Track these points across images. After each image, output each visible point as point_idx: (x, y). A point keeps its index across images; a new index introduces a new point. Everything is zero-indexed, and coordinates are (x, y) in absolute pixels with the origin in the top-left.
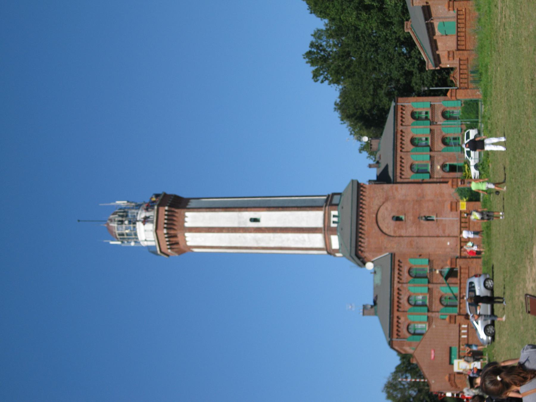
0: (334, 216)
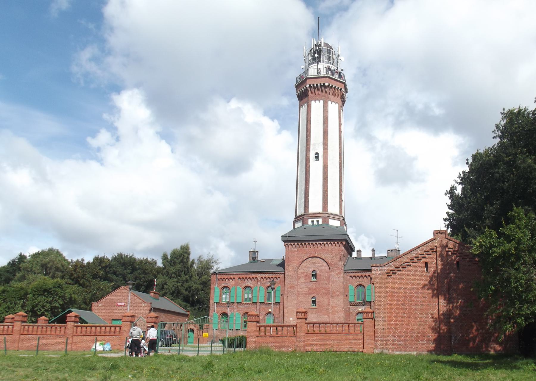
0: (318, 221)
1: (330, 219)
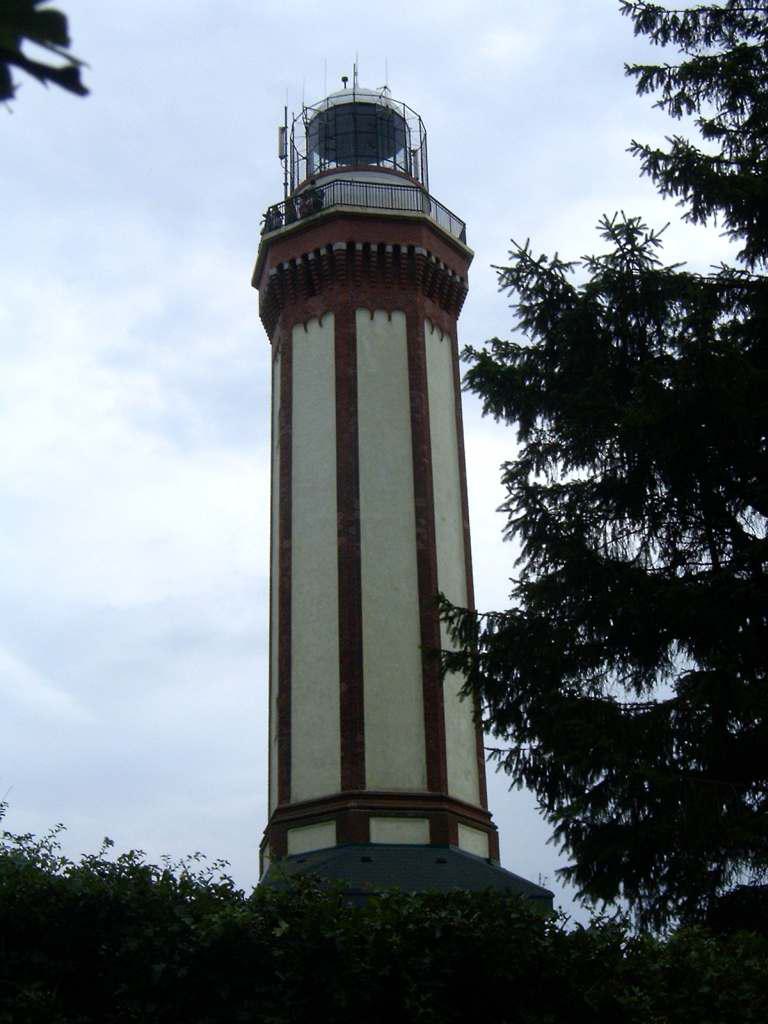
1: (459, 824)
